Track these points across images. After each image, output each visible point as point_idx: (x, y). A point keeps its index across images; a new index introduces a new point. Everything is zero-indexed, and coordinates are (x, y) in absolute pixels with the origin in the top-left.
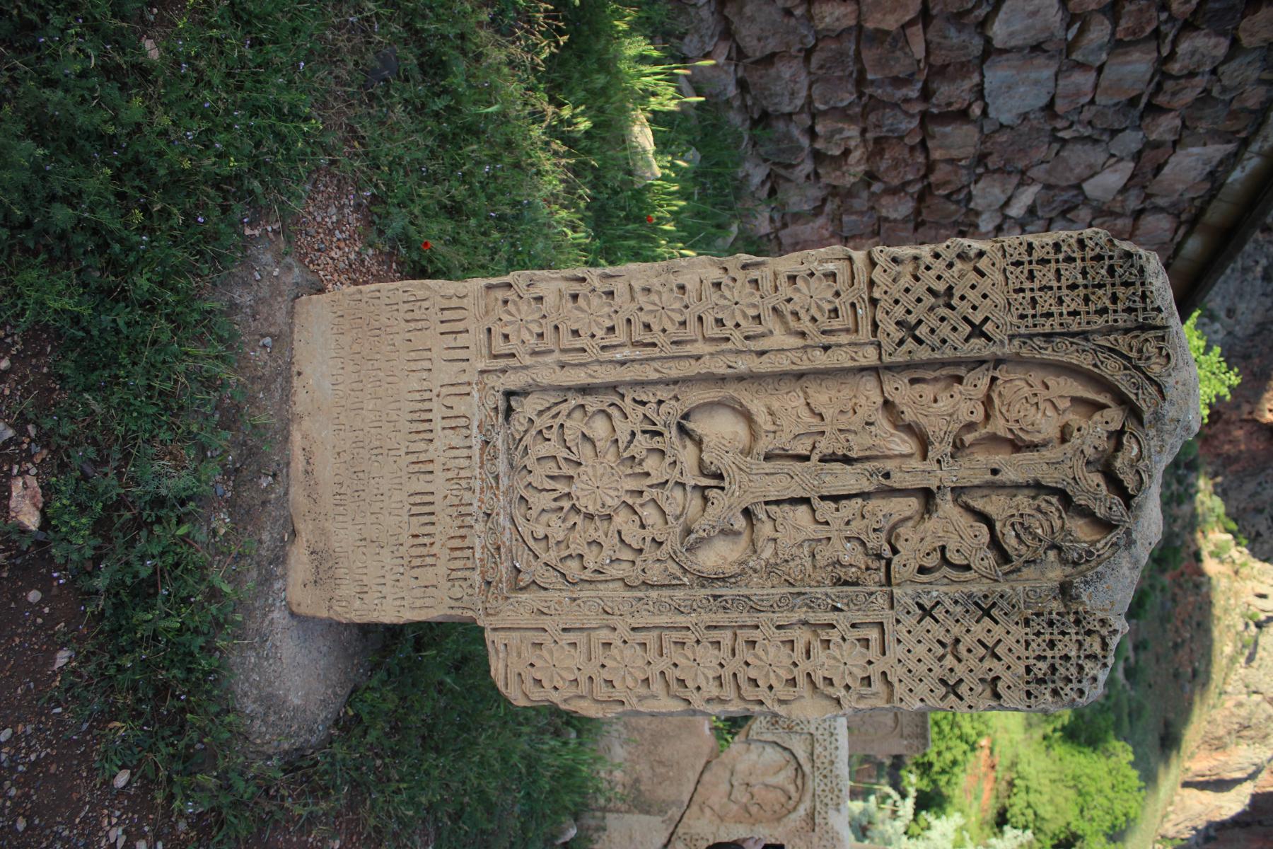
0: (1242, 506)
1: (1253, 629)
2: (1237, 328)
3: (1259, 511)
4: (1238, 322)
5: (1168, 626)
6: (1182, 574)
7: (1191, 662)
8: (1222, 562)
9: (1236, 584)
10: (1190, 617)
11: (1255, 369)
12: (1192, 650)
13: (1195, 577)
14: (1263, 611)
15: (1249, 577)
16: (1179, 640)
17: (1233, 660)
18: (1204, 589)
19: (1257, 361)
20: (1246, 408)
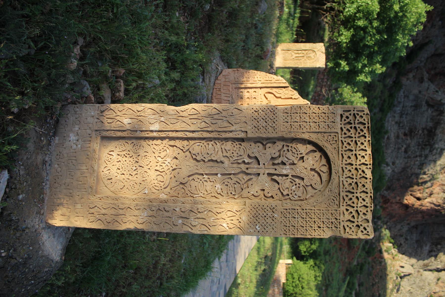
0: (396, 234)
1: (399, 279)
2: (396, 169)
3: (401, 236)
4: (396, 167)
5: (370, 277)
6: (375, 258)
7: (378, 291)
8: (389, 254)
9: (393, 262)
10: (378, 274)
11: (401, 184)
12: (378, 287)
13: (380, 259)
14: (403, 272)
15: (398, 260)
16: (374, 283)
17: (392, 290)
18: (383, 264)
19: (402, 181)
20: (398, 198)
